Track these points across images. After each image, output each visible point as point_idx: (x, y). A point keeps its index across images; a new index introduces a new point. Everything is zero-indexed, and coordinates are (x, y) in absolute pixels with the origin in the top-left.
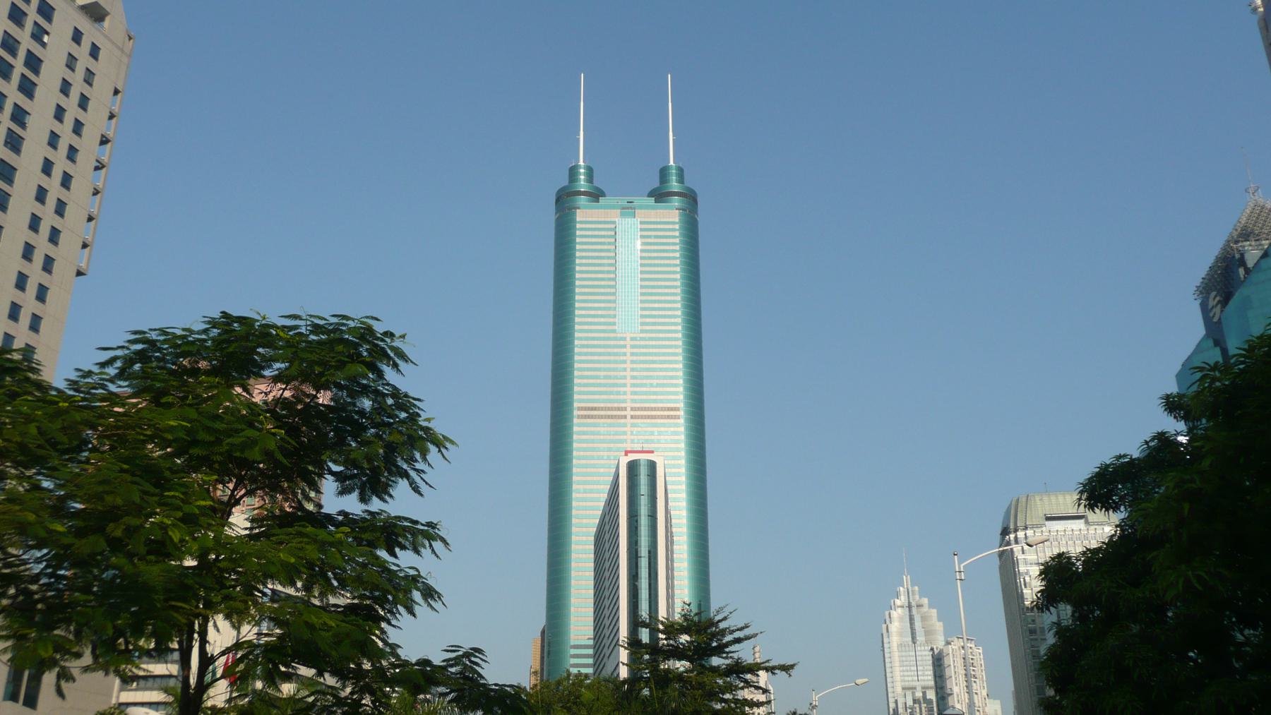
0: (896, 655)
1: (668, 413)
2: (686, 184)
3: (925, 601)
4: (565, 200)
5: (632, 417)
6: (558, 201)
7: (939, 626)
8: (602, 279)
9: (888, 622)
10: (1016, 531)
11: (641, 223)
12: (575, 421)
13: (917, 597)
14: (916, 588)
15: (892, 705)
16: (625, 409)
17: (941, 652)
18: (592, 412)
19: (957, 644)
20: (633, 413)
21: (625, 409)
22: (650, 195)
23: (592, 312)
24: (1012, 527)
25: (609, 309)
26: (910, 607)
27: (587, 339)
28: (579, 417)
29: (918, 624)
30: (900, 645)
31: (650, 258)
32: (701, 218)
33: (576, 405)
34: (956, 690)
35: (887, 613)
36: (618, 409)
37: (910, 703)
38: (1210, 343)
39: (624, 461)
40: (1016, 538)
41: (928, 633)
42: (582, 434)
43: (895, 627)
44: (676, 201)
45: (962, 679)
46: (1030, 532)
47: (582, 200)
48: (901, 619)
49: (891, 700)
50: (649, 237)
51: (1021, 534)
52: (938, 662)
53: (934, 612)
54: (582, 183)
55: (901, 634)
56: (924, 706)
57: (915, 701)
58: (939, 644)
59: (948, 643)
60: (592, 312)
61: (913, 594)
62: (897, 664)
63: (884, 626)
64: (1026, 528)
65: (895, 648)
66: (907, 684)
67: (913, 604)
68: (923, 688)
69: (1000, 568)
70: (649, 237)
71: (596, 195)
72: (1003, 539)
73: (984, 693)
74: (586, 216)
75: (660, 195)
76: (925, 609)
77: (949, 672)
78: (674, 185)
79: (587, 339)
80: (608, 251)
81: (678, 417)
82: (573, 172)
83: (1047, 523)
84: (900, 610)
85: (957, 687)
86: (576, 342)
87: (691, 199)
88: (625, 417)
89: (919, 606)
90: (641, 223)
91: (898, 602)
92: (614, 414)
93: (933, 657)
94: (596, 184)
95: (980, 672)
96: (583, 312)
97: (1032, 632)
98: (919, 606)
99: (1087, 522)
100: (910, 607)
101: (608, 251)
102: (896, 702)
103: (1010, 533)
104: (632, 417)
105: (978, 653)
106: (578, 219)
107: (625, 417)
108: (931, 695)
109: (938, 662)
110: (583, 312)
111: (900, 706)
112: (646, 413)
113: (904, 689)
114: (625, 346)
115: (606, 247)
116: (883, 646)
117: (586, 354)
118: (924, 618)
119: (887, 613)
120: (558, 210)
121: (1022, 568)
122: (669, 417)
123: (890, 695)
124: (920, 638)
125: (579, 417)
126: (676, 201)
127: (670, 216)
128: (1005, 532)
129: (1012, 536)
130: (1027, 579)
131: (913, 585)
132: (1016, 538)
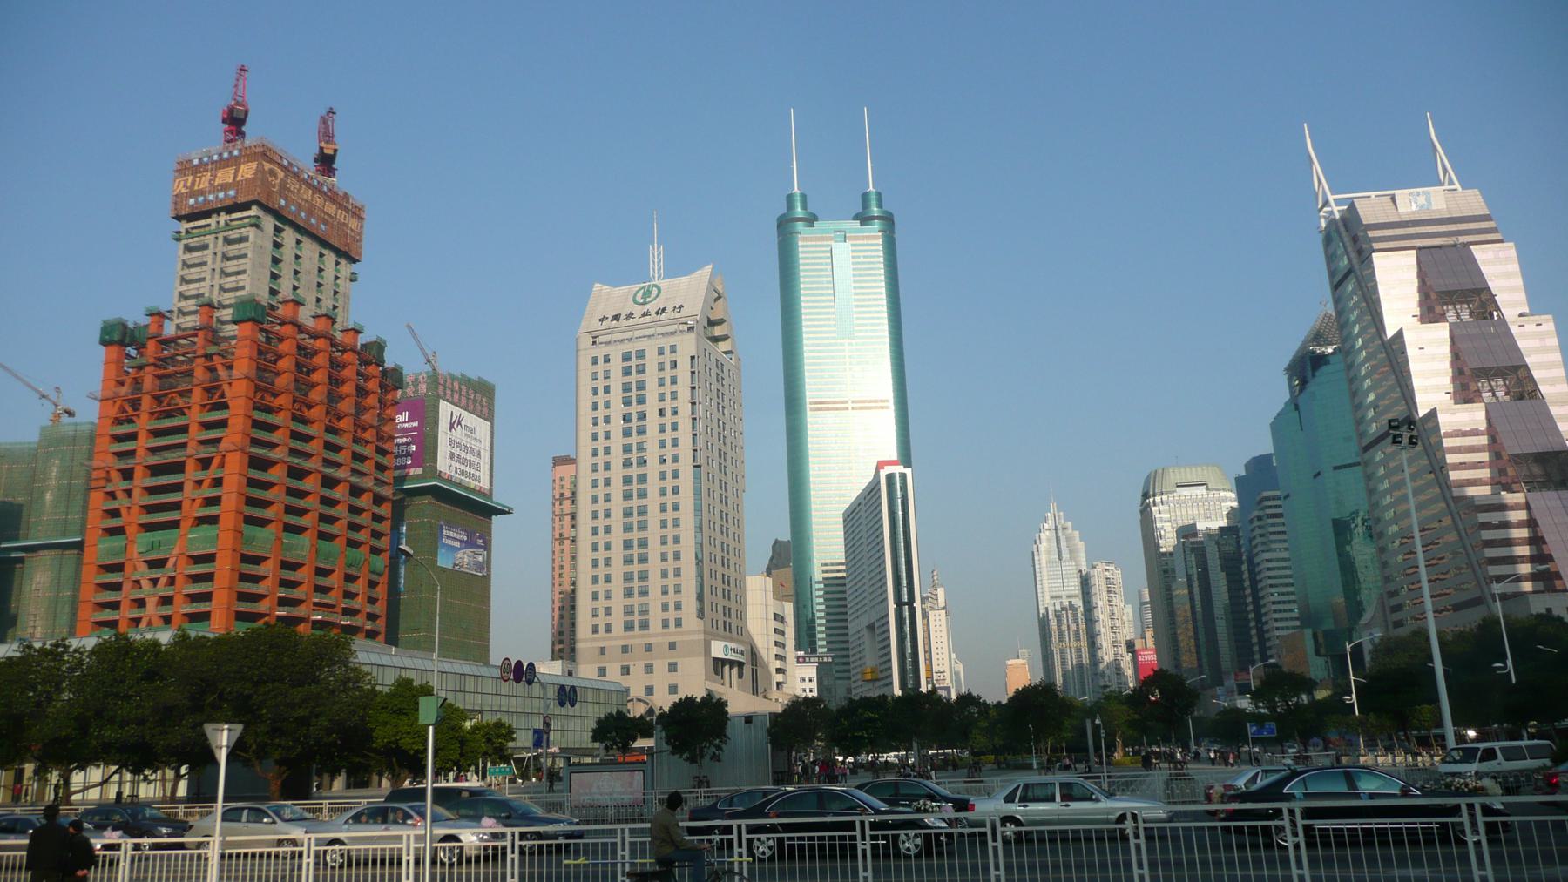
0: (1045, 570)
1: (877, 404)
2: (884, 208)
3: (1069, 524)
4: (785, 225)
5: (853, 408)
6: (778, 227)
7: (1081, 545)
8: (822, 295)
9: (1038, 542)
10: (1154, 495)
11: (853, 245)
12: (809, 413)
13: (1062, 521)
14: (1062, 514)
15: (1042, 611)
16: (847, 402)
17: (1087, 574)
18: (821, 406)
19: (1101, 567)
20: (855, 405)
21: (847, 402)
22: (856, 218)
23: (816, 323)
24: (1151, 493)
25: (829, 319)
26: (1056, 529)
27: (813, 345)
28: (811, 410)
29: (1063, 544)
30: (1049, 562)
31: (860, 275)
32: (897, 236)
33: (808, 400)
34: (1100, 603)
35: (1037, 535)
36: (842, 402)
37: (1058, 608)
38: (1293, 406)
39: (883, 474)
40: (1154, 501)
41: (1072, 551)
42: (817, 425)
43: (1043, 547)
44: (877, 225)
45: (1105, 594)
46: (1165, 497)
47: (800, 226)
48: (1049, 540)
49: (1041, 607)
50: (859, 257)
51: (1158, 499)
52: (1085, 582)
53: (1077, 533)
54: (799, 211)
55: (1048, 552)
56: (1070, 612)
57: (1062, 609)
58: (1084, 568)
59: (1094, 567)
60: (816, 323)
61: (1059, 519)
62: (1046, 578)
63: (1035, 546)
64: (1162, 494)
65: (1044, 565)
66: (1054, 594)
67: (1059, 527)
68: (1069, 597)
69: (1141, 521)
70: (859, 257)
71: (811, 220)
72: (1144, 500)
73: (1122, 604)
74: (807, 244)
75: (864, 219)
76: (1070, 531)
77: (1095, 590)
78: (875, 211)
79: (813, 345)
80: (826, 270)
81: (887, 408)
82: (790, 199)
83: (1178, 489)
84: (1047, 533)
85: (1100, 601)
86: (805, 348)
87: (888, 220)
88: (847, 409)
89: (1064, 529)
90: (853, 245)
91: (1046, 526)
92: (838, 406)
93: (1081, 577)
94: (810, 209)
95: (1119, 588)
96: (809, 323)
97: (1166, 571)
98: (1064, 529)
99: (1207, 489)
100: (1056, 529)
101: (826, 270)
102: (1047, 609)
103: (1149, 498)
104: (853, 408)
105: (1117, 573)
106: (800, 243)
107: (847, 409)
108: (1078, 602)
109: (1085, 582)
110: (809, 323)
111: (1050, 613)
112: (863, 405)
113: (1052, 598)
114: (844, 351)
115: (823, 267)
116: (1034, 566)
117: (814, 358)
118: (1068, 539)
119: (1037, 535)
120: (779, 234)
121: (1159, 525)
122: (882, 408)
123: (1040, 603)
124: (1065, 555)
125: (811, 410)
126: (877, 225)
127: (872, 241)
128: (1146, 495)
129: (1151, 500)
130: (1163, 532)
131: (1058, 512)
132: (1154, 501)
